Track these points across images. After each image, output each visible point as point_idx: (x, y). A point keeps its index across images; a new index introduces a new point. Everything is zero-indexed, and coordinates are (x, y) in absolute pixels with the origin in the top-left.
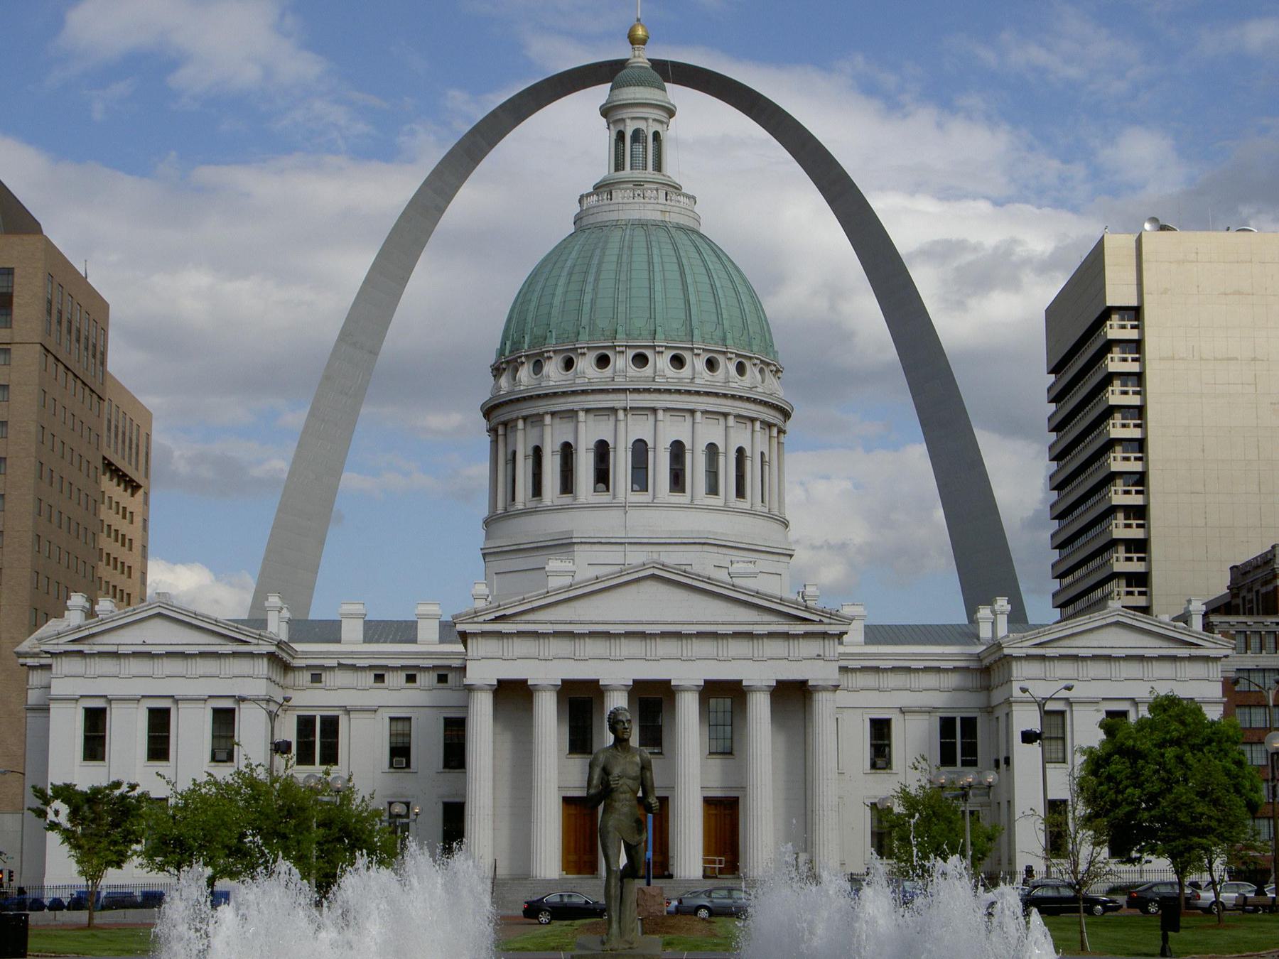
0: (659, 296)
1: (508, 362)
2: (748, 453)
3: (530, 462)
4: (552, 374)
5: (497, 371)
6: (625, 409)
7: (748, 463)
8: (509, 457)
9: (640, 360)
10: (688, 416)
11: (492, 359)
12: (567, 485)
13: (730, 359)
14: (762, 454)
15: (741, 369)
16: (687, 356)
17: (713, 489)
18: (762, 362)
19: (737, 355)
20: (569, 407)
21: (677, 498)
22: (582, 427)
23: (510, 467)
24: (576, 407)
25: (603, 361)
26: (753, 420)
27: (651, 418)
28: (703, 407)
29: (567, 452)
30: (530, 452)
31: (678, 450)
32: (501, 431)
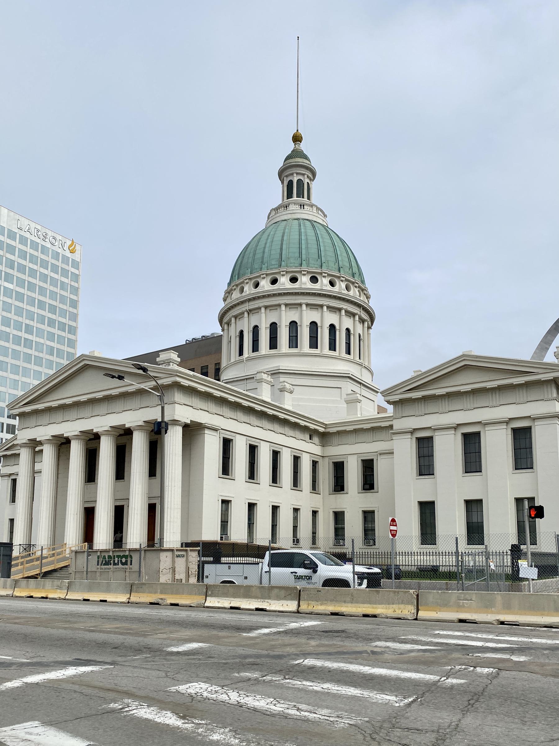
0: (322, 249)
1: (237, 286)
3: (251, 334)
4: (265, 286)
5: (229, 293)
6: (307, 305)
8: (238, 334)
9: (314, 280)
11: (226, 288)
12: (273, 344)
20: (277, 303)
22: (283, 313)
23: (238, 339)
24: (281, 302)
25: (294, 280)
29: (274, 328)
30: (251, 329)
32: (233, 320)
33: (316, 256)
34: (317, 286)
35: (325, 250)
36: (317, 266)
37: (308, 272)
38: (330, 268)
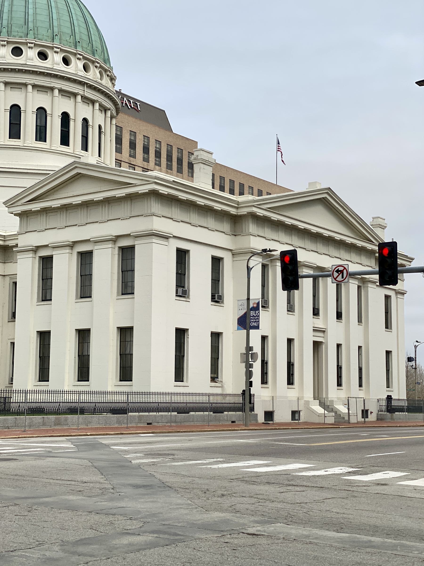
0: (31, 11)
2: (90, 123)
7: (90, 130)
10: (49, 94)
13: (79, 59)
14: (100, 127)
15: (86, 68)
16: (49, 52)
17: (65, 140)
18: (101, 67)
19: (85, 58)
21: (40, 145)
26: (93, 102)
27: (23, 89)
28: (59, 87)
31: (41, 112)
33: (22, 22)
34: (20, 60)
35: (35, 14)
36: (20, 34)
37: (8, 42)
38: (40, 37)
